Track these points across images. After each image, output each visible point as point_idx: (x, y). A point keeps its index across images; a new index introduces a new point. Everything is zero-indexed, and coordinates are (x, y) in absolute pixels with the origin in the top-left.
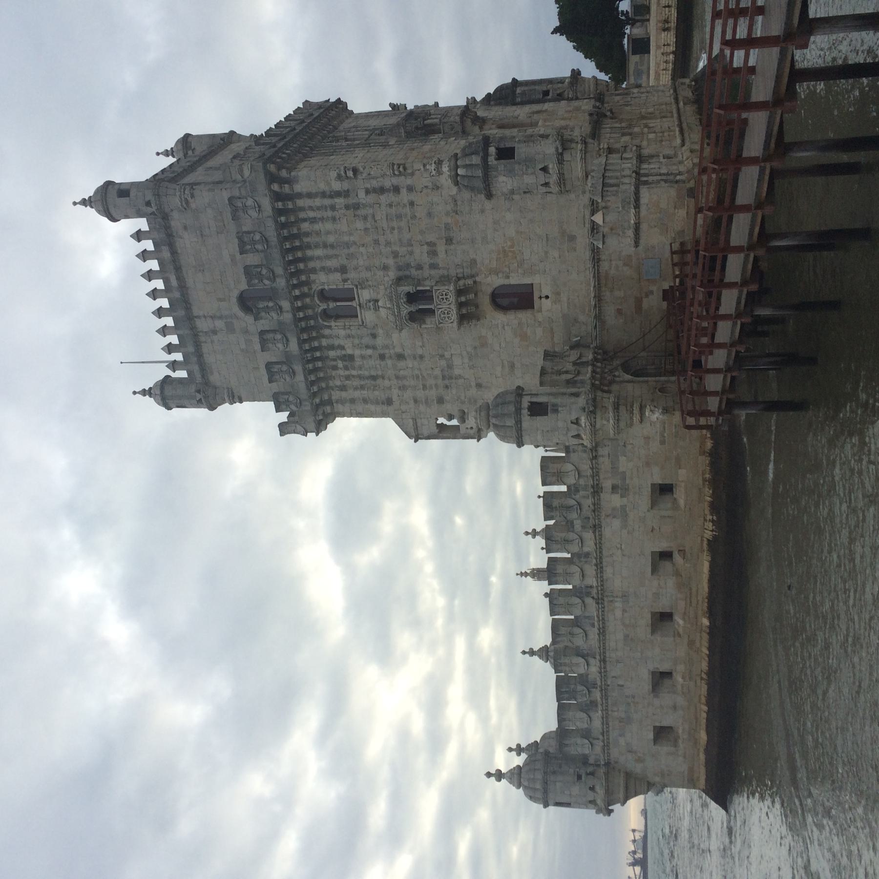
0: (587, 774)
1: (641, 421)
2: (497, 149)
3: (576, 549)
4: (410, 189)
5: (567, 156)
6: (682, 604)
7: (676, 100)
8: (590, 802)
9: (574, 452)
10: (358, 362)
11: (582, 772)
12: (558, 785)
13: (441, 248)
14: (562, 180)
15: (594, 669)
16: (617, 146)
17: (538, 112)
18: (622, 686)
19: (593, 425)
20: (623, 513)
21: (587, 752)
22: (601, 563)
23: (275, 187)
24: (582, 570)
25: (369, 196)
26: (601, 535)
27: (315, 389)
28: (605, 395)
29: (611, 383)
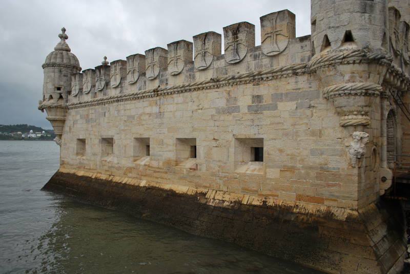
0: (60, 94)
1: (344, 126)
3: (199, 63)
6: (155, 164)
8: (44, 96)
9: (302, 47)
11: (62, 91)
12: (52, 74)
15: (113, 93)
18: (105, 116)
19: (344, 60)
20: (231, 109)
21: (73, 93)
22: (186, 91)
24: (179, 74)
26: (210, 88)
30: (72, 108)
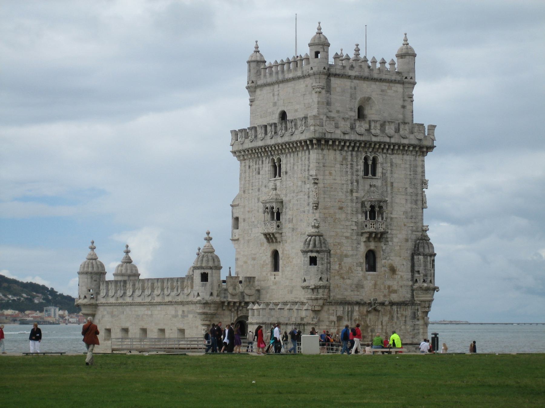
0: (92, 295)
2: (316, 258)
4: (309, 211)
5: (310, 291)
10: (257, 176)
12: (86, 280)
13: (290, 225)
14: (304, 288)
15: (129, 300)
16: (324, 315)
17: (393, 270)
19: (196, 303)
23: (308, 143)
25: (308, 190)
27: (247, 153)
28: (212, 309)
29: (230, 310)
30: (101, 306)
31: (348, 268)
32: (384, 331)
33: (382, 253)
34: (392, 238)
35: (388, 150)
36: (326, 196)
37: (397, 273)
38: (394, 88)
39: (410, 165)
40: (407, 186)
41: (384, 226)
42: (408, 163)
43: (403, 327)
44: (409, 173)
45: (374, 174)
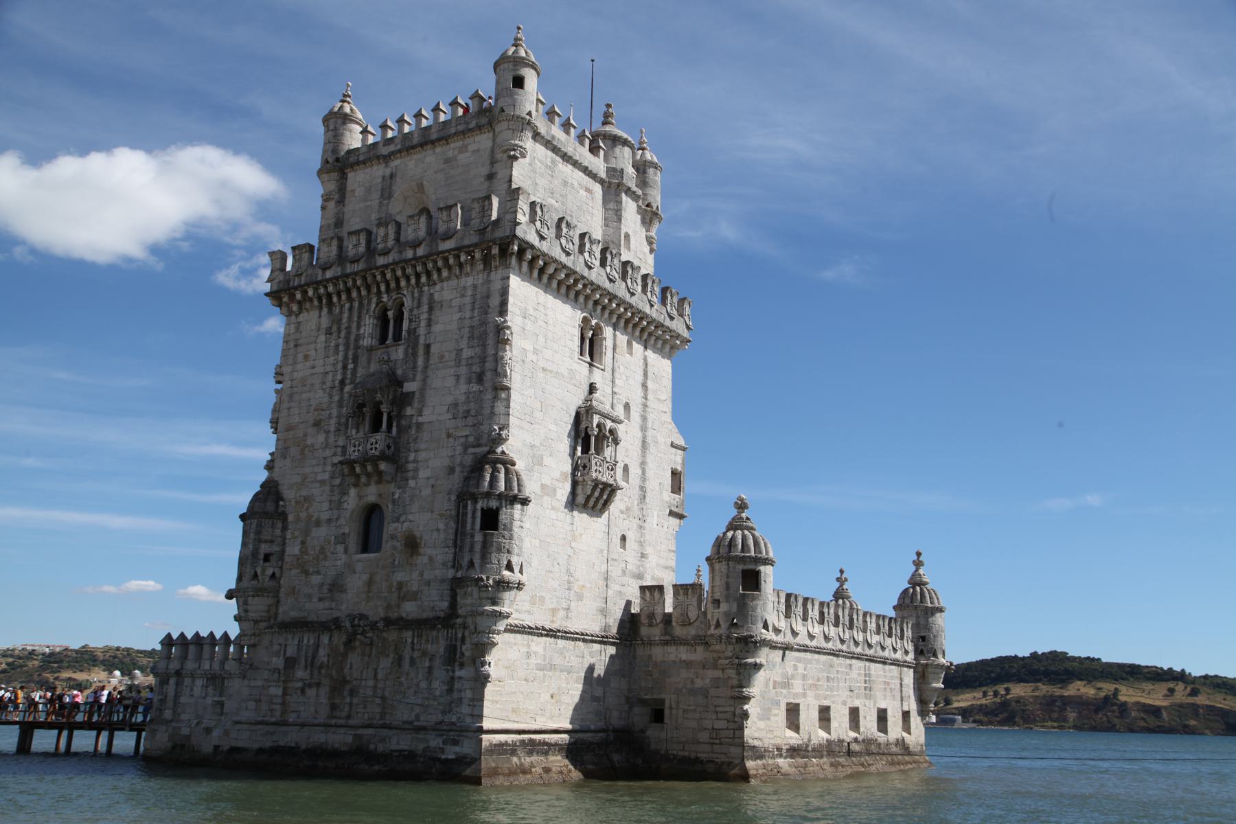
7: (389, 727)
17: (412, 545)
31: (318, 548)
32: (379, 693)
33: (390, 506)
34: (416, 470)
35: (418, 276)
36: (292, 404)
37: (422, 551)
38: (471, 148)
39: (474, 296)
40: (464, 344)
41: (380, 446)
42: (469, 292)
43: (423, 685)
44: (468, 314)
45: (397, 337)
